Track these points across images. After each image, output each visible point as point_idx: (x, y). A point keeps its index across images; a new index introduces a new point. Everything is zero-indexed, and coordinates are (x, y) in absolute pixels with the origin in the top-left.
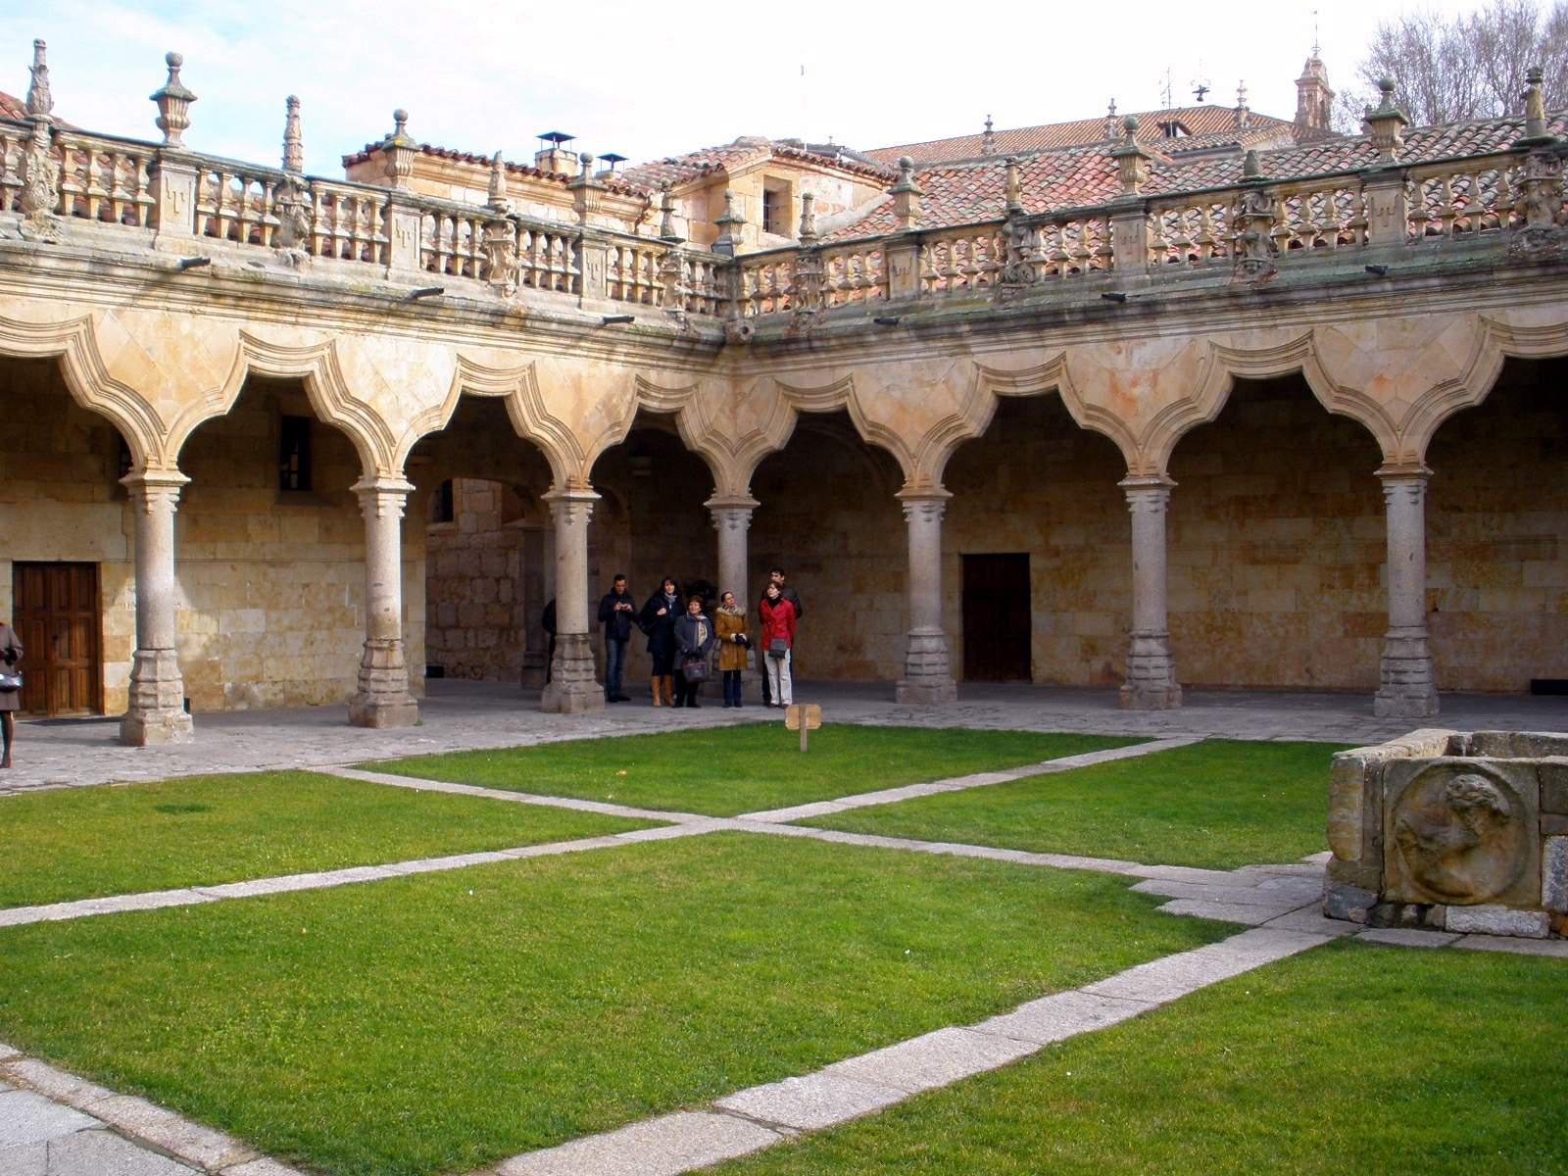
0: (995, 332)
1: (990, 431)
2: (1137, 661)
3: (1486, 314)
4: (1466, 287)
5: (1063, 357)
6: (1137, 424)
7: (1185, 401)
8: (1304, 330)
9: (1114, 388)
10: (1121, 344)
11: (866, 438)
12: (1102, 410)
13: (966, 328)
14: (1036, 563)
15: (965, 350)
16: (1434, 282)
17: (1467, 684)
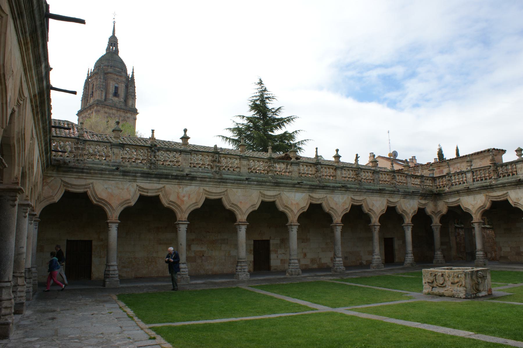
0: (147, 177)
1: (201, 207)
2: (111, 272)
3: (261, 191)
4: (260, 185)
5: (164, 187)
6: (184, 207)
7: (196, 202)
8: (226, 189)
9: (178, 197)
10: (181, 186)
11: (95, 202)
12: (174, 203)
13: (140, 175)
14: (94, 243)
15: (135, 180)
16: (255, 183)
17: (210, 273)
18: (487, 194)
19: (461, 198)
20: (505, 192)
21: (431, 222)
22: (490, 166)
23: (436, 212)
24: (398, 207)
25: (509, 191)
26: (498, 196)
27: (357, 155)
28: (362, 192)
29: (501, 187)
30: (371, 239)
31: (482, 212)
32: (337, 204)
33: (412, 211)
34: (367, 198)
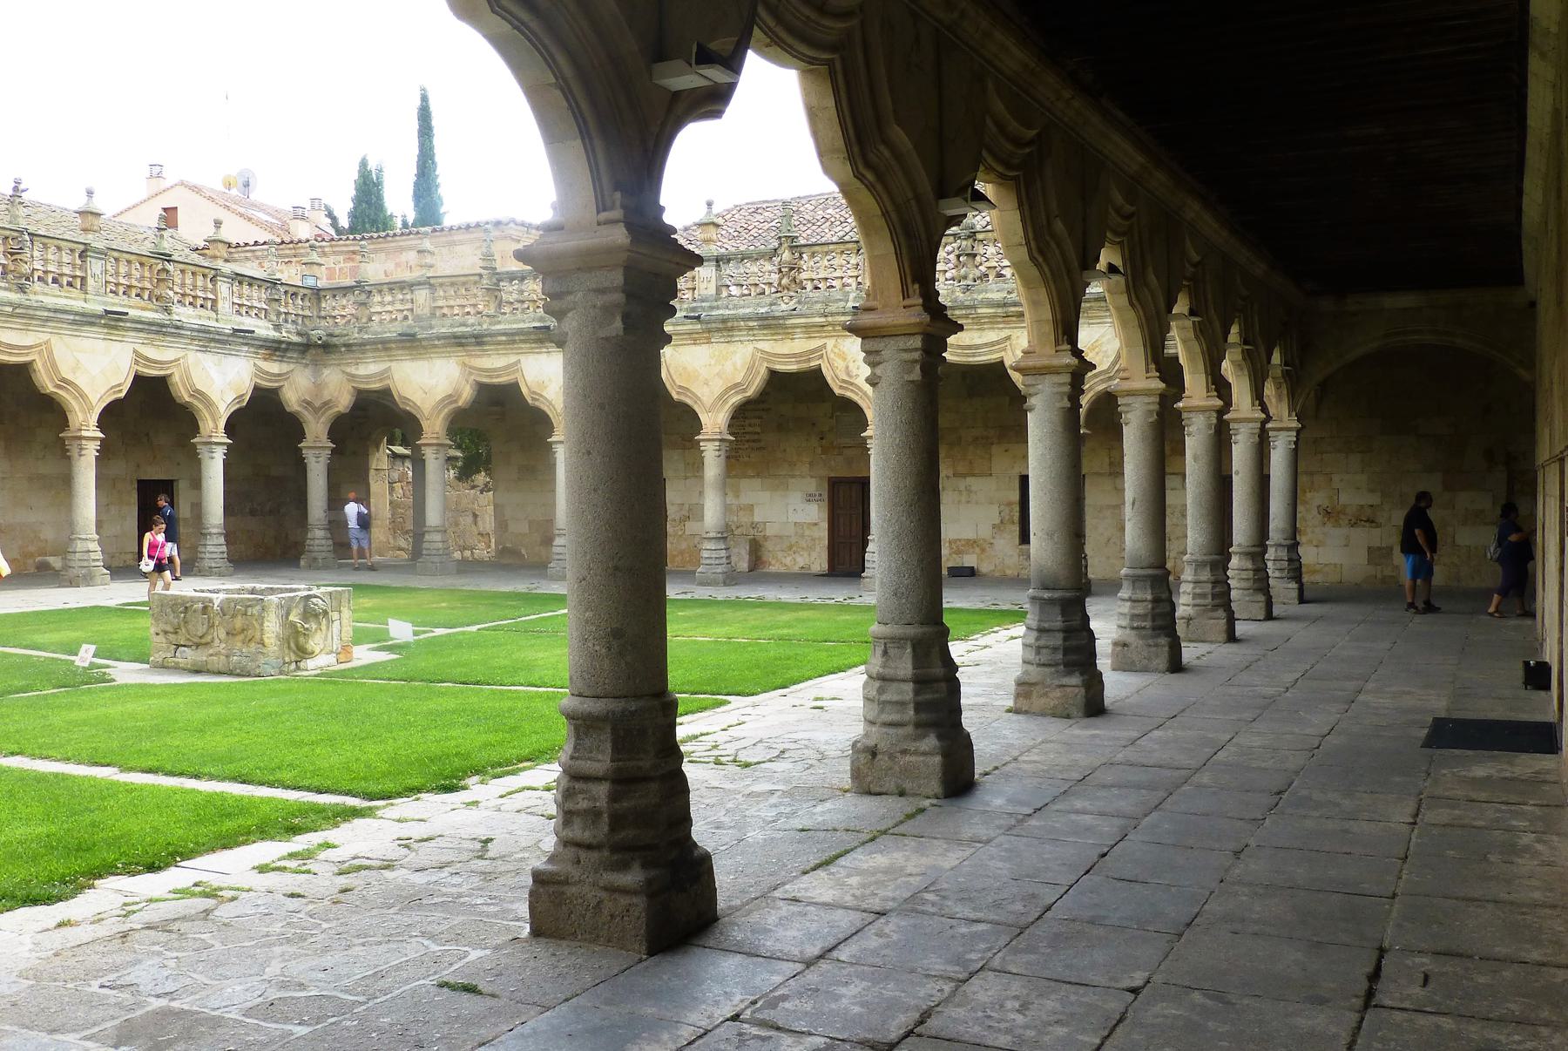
19: (394, 365)
20: (513, 359)
21: (301, 435)
22: (481, 276)
23: (317, 404)
24: (176, 378)
25: (522, 358)
26: (495, 370)
27: (18, 182)
28: (32, 317)
30: (66, 482)
31: (448, 415)
33: (230, 396)
34: (54, 340)
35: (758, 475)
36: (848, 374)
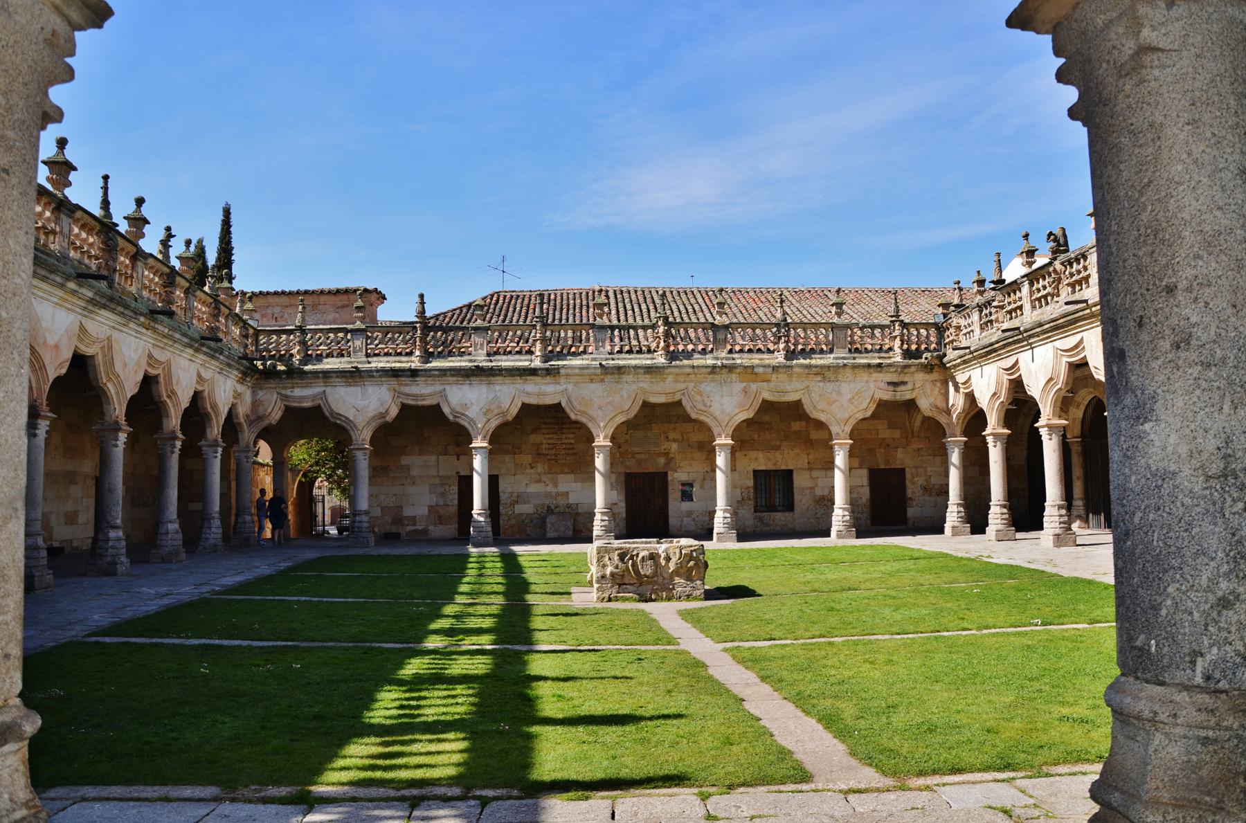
18: (397, 387)
19: (328, 390)
20: (439, 388)
23: (253, 418)
25: (447, 388)
29: (439, 376)
32: (125, 364)
35: (572, 472)
36: (705, 405)
